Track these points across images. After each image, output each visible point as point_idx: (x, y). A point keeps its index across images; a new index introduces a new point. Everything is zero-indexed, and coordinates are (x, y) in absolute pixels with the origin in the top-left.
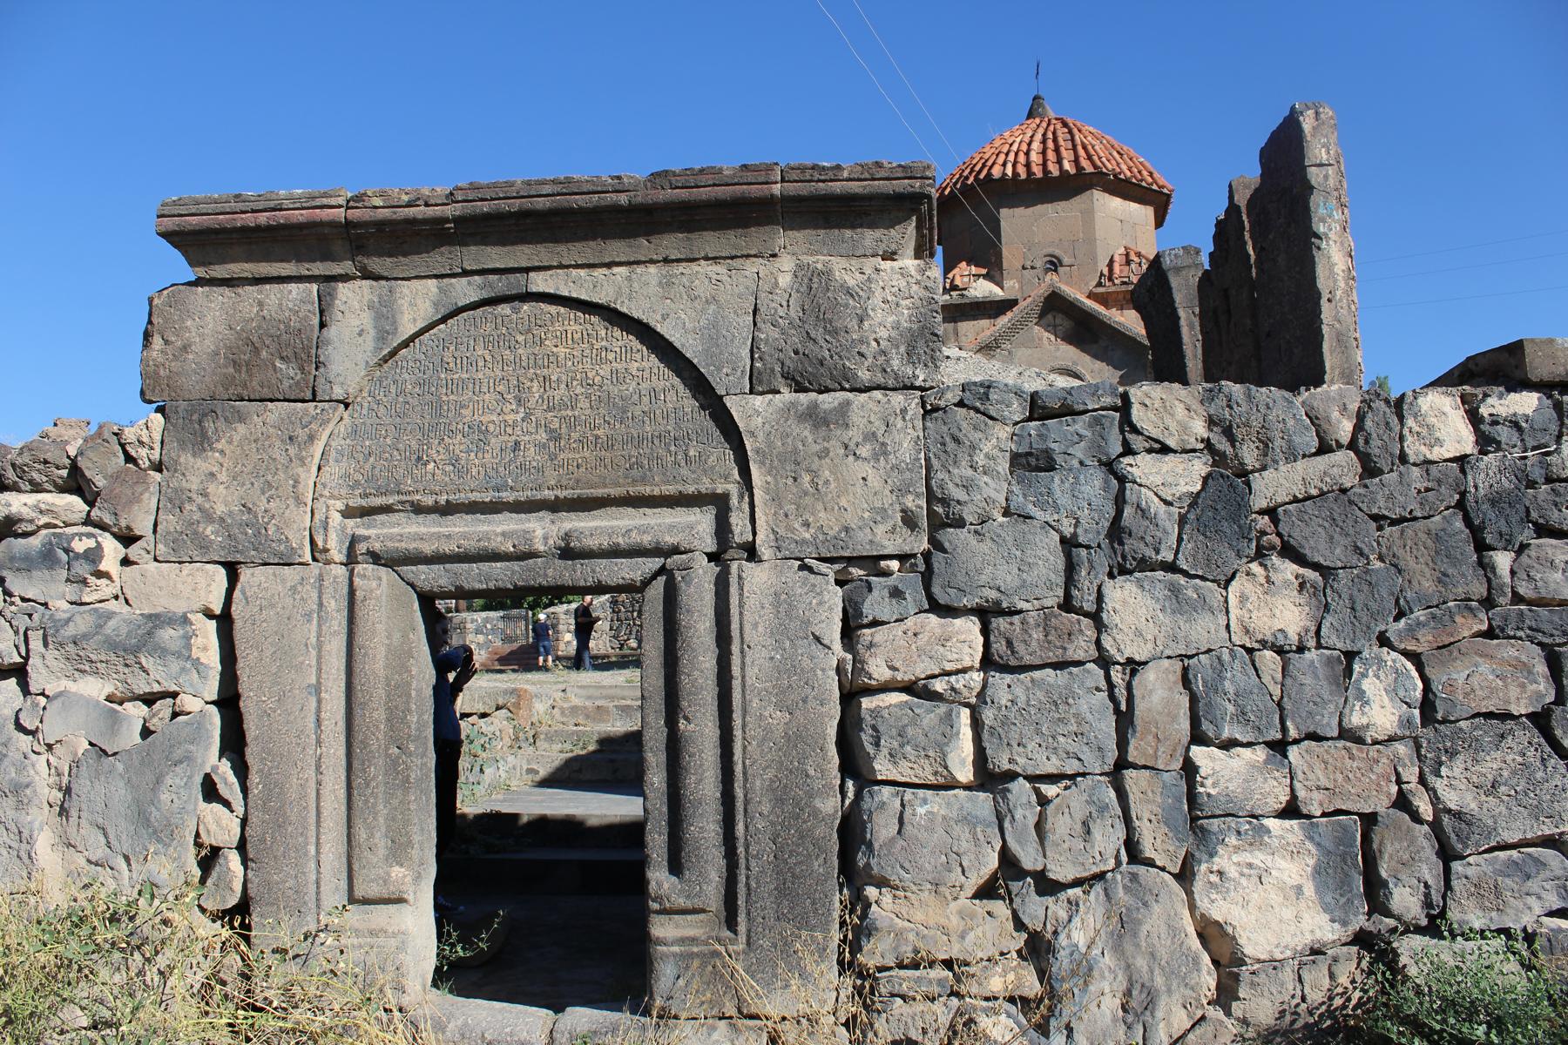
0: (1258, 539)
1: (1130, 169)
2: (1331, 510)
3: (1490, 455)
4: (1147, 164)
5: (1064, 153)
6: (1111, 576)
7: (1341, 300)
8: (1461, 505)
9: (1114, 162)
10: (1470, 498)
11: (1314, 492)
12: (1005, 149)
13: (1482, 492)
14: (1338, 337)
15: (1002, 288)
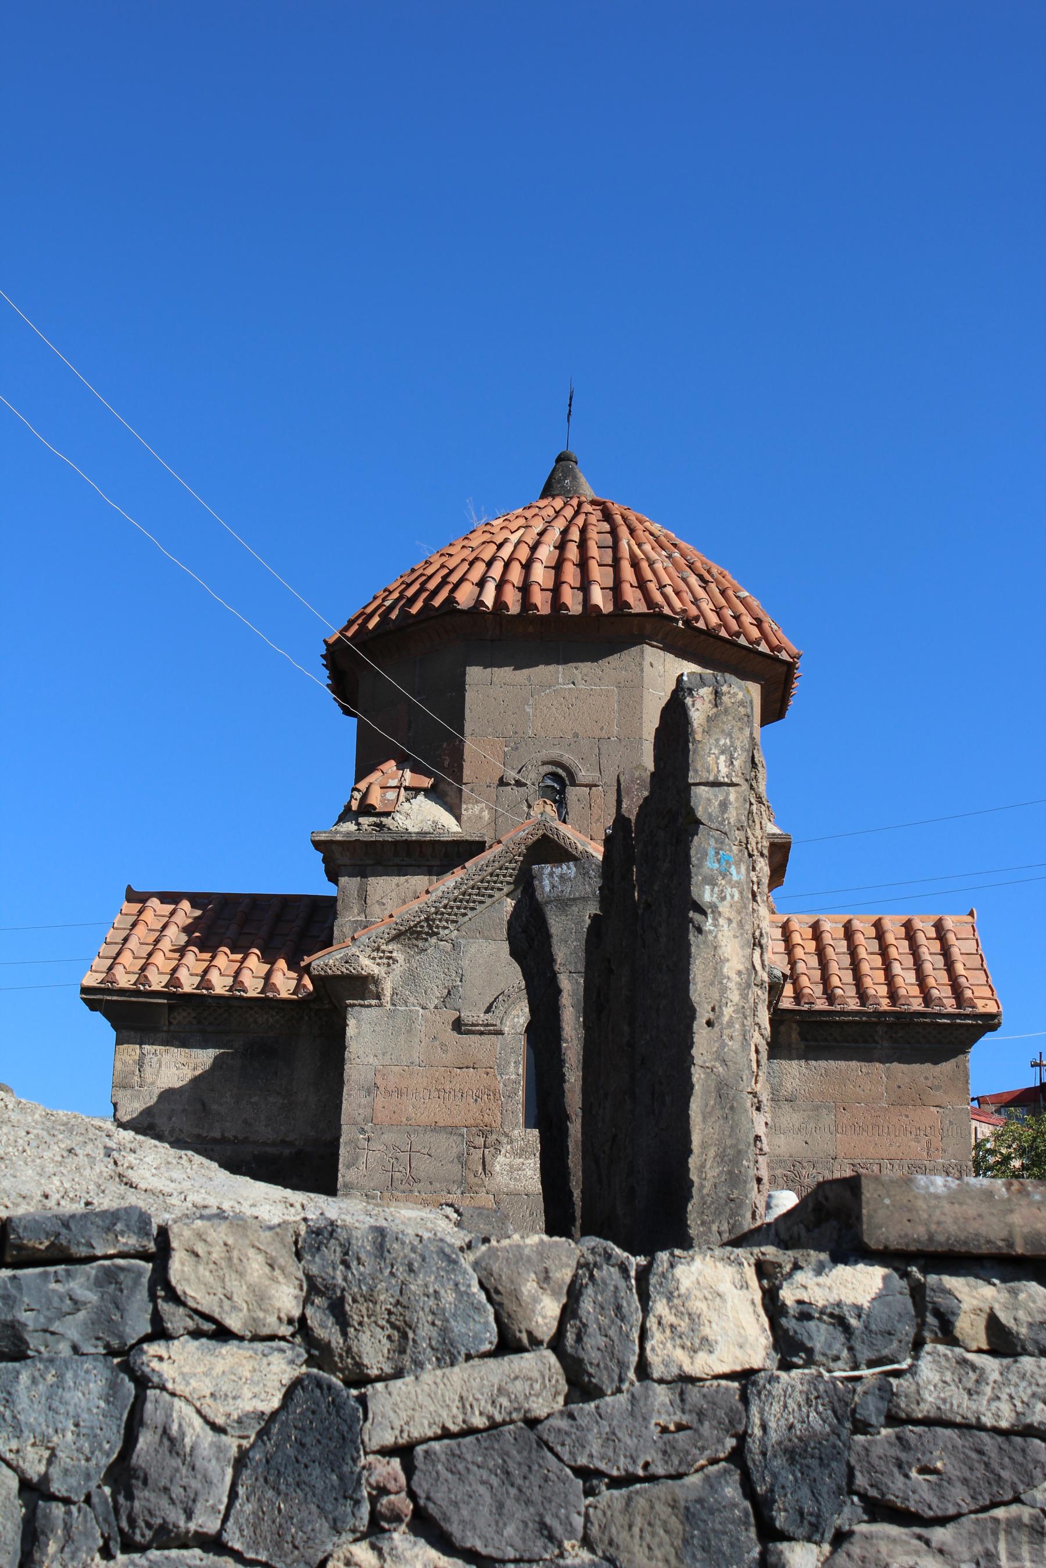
0: (373, 1500)
1: (718, 611)
2: (505, 1454)
3: (795, 1373)
4: (755, 603)
5: (596, 572)
6: (107, 1554)
7: (730, 1024)
8: (738, 1456)
9: (687, 597)
10: (754, 1446)
11: (479, 1422)
12: (487, 554)
13: (774, 1436)
14: (719, 1090)
15: (458, 818)
